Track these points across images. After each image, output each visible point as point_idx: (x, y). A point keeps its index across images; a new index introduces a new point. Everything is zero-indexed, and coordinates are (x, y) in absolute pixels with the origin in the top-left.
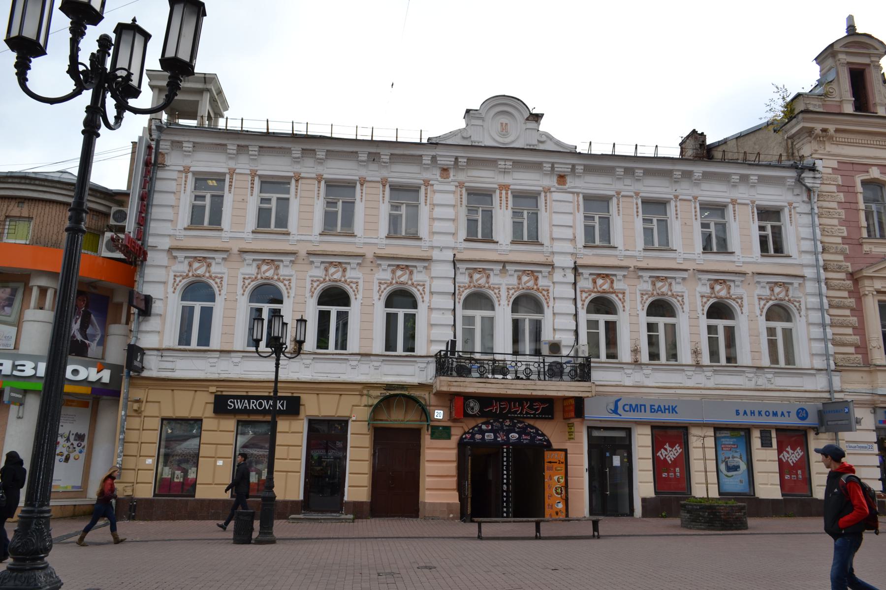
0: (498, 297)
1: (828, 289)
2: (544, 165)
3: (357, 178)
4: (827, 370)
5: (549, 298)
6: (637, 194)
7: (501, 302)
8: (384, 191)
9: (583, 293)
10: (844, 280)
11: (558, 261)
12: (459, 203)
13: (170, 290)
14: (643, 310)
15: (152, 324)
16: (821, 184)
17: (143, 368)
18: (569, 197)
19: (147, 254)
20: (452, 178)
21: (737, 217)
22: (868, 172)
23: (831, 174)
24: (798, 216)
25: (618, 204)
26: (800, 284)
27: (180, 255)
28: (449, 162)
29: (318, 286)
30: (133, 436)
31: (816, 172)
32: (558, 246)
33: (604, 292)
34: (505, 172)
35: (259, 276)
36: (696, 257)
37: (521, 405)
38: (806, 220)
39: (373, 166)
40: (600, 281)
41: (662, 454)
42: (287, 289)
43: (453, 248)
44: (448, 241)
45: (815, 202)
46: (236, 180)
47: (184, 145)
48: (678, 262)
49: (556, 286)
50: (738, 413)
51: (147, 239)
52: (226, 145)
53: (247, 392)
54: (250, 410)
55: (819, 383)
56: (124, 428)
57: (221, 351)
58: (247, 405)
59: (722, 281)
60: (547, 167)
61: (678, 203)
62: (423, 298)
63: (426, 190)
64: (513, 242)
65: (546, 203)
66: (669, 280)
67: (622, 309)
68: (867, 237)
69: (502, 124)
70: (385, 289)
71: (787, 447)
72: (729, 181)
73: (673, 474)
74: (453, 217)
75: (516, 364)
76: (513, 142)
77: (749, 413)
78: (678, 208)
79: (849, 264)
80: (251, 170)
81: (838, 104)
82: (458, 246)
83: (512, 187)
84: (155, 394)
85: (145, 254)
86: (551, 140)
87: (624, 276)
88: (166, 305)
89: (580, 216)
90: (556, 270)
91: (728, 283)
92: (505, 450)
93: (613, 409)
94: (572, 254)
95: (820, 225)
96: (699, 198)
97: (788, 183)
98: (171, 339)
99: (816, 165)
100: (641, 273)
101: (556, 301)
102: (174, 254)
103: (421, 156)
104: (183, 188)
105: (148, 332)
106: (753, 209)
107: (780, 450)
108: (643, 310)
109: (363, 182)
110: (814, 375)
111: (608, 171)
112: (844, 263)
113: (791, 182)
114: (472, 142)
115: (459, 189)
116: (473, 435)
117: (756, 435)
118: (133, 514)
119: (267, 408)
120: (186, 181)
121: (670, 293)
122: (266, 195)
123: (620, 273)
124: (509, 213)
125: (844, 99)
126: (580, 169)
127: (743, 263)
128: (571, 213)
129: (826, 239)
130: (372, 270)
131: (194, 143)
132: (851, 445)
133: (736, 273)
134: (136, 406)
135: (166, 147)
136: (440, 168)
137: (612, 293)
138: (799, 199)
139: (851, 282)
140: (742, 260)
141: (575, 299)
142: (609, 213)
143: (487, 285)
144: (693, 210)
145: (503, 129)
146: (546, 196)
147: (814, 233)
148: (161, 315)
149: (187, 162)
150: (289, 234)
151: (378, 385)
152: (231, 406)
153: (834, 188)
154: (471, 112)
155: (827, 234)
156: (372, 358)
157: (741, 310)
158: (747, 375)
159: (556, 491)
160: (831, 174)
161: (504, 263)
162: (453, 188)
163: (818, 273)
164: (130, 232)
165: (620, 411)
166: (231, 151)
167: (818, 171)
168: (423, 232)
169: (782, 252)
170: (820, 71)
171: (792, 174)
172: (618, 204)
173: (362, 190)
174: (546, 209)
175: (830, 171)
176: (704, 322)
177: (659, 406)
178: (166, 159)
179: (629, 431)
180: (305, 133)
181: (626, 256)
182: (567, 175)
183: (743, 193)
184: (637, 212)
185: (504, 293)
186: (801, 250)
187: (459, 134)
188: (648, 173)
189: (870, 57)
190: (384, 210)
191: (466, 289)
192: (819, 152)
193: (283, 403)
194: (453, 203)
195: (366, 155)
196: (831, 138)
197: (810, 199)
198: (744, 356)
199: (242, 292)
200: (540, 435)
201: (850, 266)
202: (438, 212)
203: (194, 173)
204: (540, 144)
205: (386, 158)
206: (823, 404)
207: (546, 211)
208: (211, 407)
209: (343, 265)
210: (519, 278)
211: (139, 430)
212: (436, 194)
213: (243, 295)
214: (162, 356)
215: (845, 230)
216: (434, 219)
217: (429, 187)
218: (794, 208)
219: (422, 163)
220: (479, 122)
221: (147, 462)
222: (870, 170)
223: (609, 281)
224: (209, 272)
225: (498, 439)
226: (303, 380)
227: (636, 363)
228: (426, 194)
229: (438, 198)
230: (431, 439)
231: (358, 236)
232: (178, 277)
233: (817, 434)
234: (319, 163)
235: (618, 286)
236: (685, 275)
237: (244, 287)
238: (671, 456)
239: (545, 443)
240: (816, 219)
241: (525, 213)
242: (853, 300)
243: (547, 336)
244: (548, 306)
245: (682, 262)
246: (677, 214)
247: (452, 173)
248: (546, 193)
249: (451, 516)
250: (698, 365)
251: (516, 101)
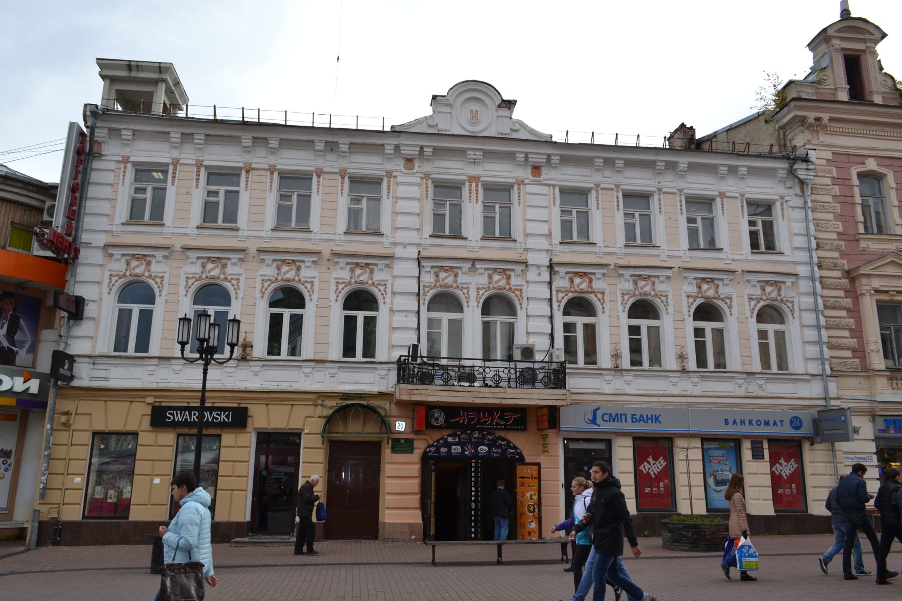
0: (466, 298)
1: (823, 288)
2: (517, 155)
3: (313, 169)
4: (822, 375)
5: (522, 299)
6: (617, 186)
7: (470, 303)
8: (342, 183)
9: (560, 293)
10: (840, 279)
11: (532, 258)
12: (425, 196)
13: (105, 290)
14: (624, 311)
15: (84, 328)
16: (813, 176)
17: (72, 377)
18: (545, 190)
19: (79, 251)
20: (417, 169)
21: (725, 211)
22: (864, 164)
23: (825, 166)
24: (790, 210)
25: (597, 198)
26: (793, 283)
27: (117, 253)
28: (414, 152)
29: (269, 286)
30: (60, 452)
31: (809, 163)
32: (532, 243)
33: (582, 292)
34: (475, 162)
35: (204, 276)
36: (681, 254)
37: (491, 414)
38: (799, 214)
39: (331, 157)
40: (577, 281)
41: (645, 467)
42: (235, 289)
43: (418, 245)
44: (413, 237)
45: (808, 196)
46: (180, 171)
47: (123, 133)
48: (662, 259)
49: (530, 285)
50: (726, 422)
51: (79, 236)
52: (168, 133)
53: (189, 403)
54: (191, 422)
55: (814, 389)
56: (49, 443)
57: (160, 358)
58: (188, 417)
59: (709, 280)
60: (520, 157)
61: (662, 197)
62: (384, 299)
63: (389, 182)
64: (483, 239)
65: (519, 196)
66: (652, 279)
67: (602, 310)
68: (864, 232)
69: (471, 111)
70: (343, 289)
71: (780, 459)
72: (716, 173)
73: (657, 489)
74: (419, 212)
75: (484, 370)
76: (483, 130)
77: (738, 422)
78: (662, 202)
79: (845, 262)
80: (197, 161)
81: (832, 91)
82: (423, 242)
83: (482, 179)
84: (85, 406)
85: (77, 252)
86: (525, 128)
87: (604, 275)
88: (100, 308)
89: (556, 211)
90: (530, 269)
91: (716, 282)
92: (473, 465)
93: (591, 419)
94: (547, 251)
95: (814, 220)
96: (685, 191)
97: (780, 175)
98: (105, 343)
99: (809, 156)
100: (621, 272)
101: (530, 302)
102: (109, 252)
103: (383, 145)
104: (121, 180)
105: (79, 337)
106: (742, 202)
107: (773, 462)
108: (624, 311)
109: (320, 173)
110: (808, 380)
111: (587, 162)
112: (839, 261)
113: (782, 174)
114: (439, 130)
115: (425, 181)
116: (438, 448)
117: (746, 446)
118: (58, 539)
119: (210, 420)
120: (124, 172)
121: (653, 293)
122: (213, 188)
123: (599, 272)
124: (479, 207)
125: (838, 86)
126: (555, 160)
127: (732, 260)
128: (547, 207)
129: (821, 235)
130: (329, 269)
131: (134, 130)
132: (848, 456)
133: (725, 271)
134: (63, 419)
135: (102, 135)
136: (404, 158)
137: (591, 293)
138: (791, 192)
139: (848, 281)
140: (731, 257)
141: (551, 300)
142: (587, 207)
143: (454, 285)
144: (678, 204)
145: (473, 117)
146: (519, 189)
147: (808, 228)
148: (94, 319)
149: (126, 151)
150: (237, 230)
151: (334, 394)
152: (170, 418)
153: (828, 181)
154: (438, 98)
155: (821, 229)
156: (328, 364)
157: (730, 311)
159: (528, 509)
160: (825, 166)
161: (474, 261)
162: (418, 180)
163: (812, 271)
164: (58, 227)
166: (175, 140)
167: (811, 162)
168: (385, 226)
169: (774, 249)
170: (814, 58)
171: (784, 165)
172: (597, 198)
173: (318, 182)
174: (519, 202)
175: (824, 162)
176: (690, 324)
177: (642, 416)
178: (103, 148)
179: (609, 442)
180: (257, 120)
181: (606, 254)
182: (542, 166)
183: (731, 186)
184: (618, 206)
185: (473, 294)
186: (794, 247)
187: (425, 122)
188: (629, 164)
189: (865, 42)
190: (343, 203)
191: (432, 289)
192: (813, 142)
193: (228, 414)
194: (418, 196)
195: (323, 144)
196: (825, 127)
197: (803, 192)
198: (734, 362)
199: (185, 293)
200: (512, 448)
201: (846, 264)
202: (402, 206)
203: (134, 164)
204: (513, 133)
205: (344, 148)
206: (819, 412)
207: (519, 205)
208: (148, 419)
209: (297, 264)
210: (490, 278)
211: (67, 445)
212: (400, 186)
213: (186, 296)
214: (94, 364)
215: (841, 225)
216: (397, 214)
217: (392, 179)
218: (787, 202)
219: (384, 153)
220: (447, 109)
221: (75, 481)
222: (867, 162)
223: (587, 280)
224: (149, 271)
225: (466, 453)
226: (251, 389)
227: (617, 369)
228: (389, 186)
229: (402, 191)
230: (392, 453)
231: (314, 232)
232: (114, 276)
233: (812, 444)
234: (272, 152)
235: (597, 285)
236: (669, 273)
237: (187, 288)
238: (655, 470)
239: (517, 457)
240: (810, 214)
241: (497, 206)
242: (849, 300)
243: (520, 339)
244: (521, 308)
245: (666, 260)
246: (660, 208)
247: (417, 163)
248: (519, 185)
249: (413, 537)
250: (684, 371)
251: (487, 86)
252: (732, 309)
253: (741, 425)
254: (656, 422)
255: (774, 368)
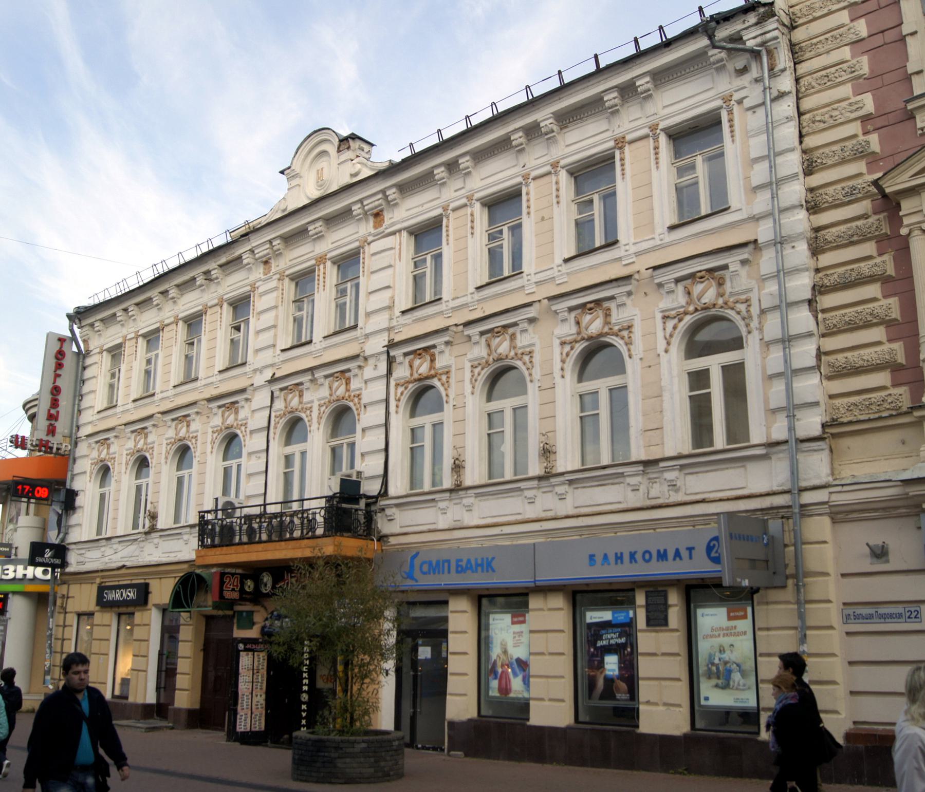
48: (558, 282)
66: (511, 331)
87: (447, 343)
155: (822, 126)
157: (629, 350)
158: (628, 480)
161: (311, 370)
165: (417, 574)
177: (469, 561)
218: (740, 102)
235: (440, 362)
236: (531, 312)
247: (272, 261)
252: (632, 347)
253: (616, 563)
254: (487, 571)
255: (720, 440)
